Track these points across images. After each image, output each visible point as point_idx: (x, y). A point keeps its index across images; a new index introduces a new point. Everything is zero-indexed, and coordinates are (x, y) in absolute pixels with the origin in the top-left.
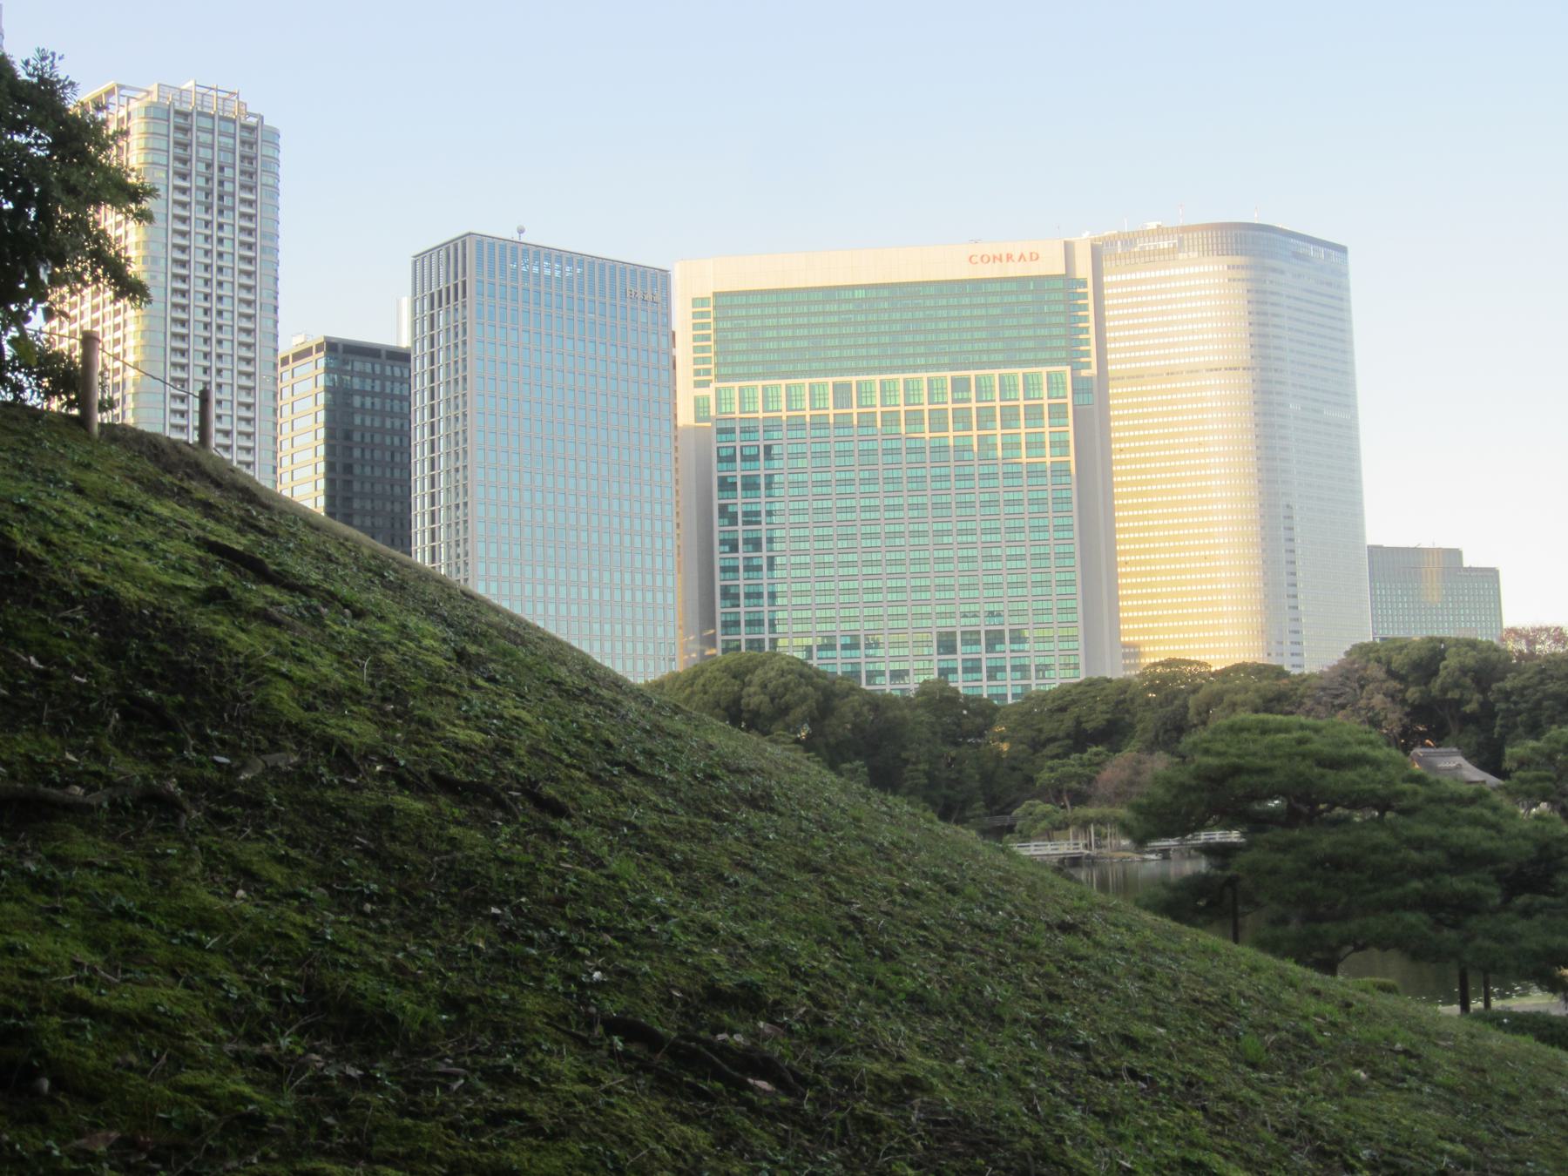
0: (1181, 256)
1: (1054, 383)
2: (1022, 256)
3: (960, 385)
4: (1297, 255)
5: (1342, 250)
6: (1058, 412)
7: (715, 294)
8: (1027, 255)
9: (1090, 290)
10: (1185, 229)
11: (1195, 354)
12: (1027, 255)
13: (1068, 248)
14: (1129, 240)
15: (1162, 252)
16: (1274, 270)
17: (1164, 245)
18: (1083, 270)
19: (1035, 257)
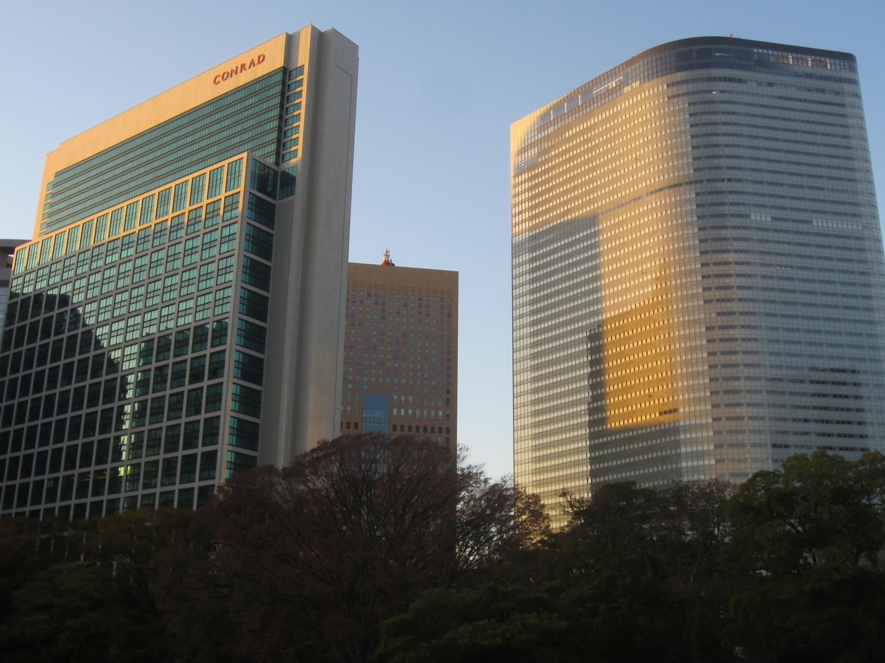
0: (627, 89)
1: (233, 175)
2: (252, 63)
3: (163, 199)
4: (762, 64)
5: (847, 59)
6: (231, 204)
7: (57, 175)
8: (256, 62)
9: (305, 77)
10: (629, 63)
11: (637, 182)
12: (256, 62)
13: (291, 42)
14: (586, 89)
15: (610, 92)
16: (725, 79)
17: (613, 84)
18: (303, 57)
19: (261, 59)
